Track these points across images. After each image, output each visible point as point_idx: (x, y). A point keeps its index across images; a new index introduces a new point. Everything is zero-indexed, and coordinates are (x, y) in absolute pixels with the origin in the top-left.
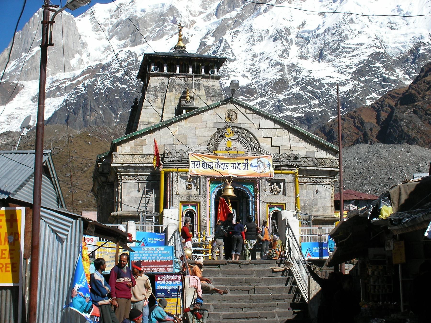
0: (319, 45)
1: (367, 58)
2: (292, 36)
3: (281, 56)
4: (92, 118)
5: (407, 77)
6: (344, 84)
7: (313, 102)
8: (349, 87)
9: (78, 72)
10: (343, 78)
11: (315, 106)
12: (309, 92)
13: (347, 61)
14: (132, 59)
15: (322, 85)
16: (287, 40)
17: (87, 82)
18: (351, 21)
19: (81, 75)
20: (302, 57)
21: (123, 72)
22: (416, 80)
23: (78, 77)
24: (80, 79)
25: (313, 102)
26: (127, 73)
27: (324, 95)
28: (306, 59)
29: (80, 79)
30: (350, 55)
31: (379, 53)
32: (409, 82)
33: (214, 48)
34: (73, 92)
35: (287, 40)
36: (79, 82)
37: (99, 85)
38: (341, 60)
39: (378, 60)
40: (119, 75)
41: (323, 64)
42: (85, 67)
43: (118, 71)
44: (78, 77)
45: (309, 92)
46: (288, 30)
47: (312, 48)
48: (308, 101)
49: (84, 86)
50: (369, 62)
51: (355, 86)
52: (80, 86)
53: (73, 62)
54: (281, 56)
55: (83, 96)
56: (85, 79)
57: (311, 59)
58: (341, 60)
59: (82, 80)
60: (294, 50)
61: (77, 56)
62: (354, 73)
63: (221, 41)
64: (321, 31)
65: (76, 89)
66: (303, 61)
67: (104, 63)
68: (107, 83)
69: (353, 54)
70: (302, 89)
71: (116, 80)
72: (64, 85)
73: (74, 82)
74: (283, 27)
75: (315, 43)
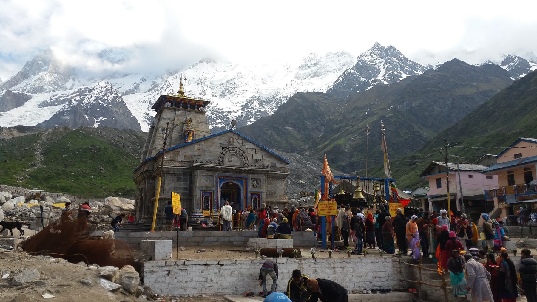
0: (222, 89)
1: (249, 99)
2: (208, 83)
3: (201, 94)
4: (81, 121)
5: (270, 110)
6: (236, 112)
7: (218, 121)
8: (239, 114)
9: (72, 91)
10: (235, 109)
11: (219, 123)
12: (216, 115)
13: (238, 100)
14: (109, 87)
15: (223, 112)
16: (205, 85)
17: (78, 98)
18: (242, 77)
19: (73, 93)
20: (213, 96)
21: (103, 94)
22: (276, 113)
23: (71, 94)
24: (73, 96)
25: (218, 121)
26: (105, 95)
27: (224, 117)
28: (215, 96)
29: (73, 96)
30: (241, 96)
31: (256, 97)
32: (272, 113)
33: (161, 86)
34: (68, 103)
35: (205, 85)
36: (72, 98)
37: (86, 101)
38: (235, 98)
39: (255, 100)
40: (100, 96)
41: (225, 100)
42: (76, 88)
43: (99, 93)
44: (71, 94)
45: (216, 115)
46: (205, 79)
47: (218, 91)
48: (215, 121)
49: (75, 100)
50: (250, 101)
51: (242, 113)
52: (73, 100)
53: (68, 85)
54: (201, 94)
55: (74, 107)
56: (77, 96)
57: (218, 97)
58: (235, 98)
59: (74, 97)
60: (209, 91)
61: (71, 81)
62: (242, 106)
63: (166, 82)
64: (224, 81)
65: (70, 102)
66: (214, 97)
67: (89, 87)
68: (92, 100)
69: (242, 95)
70: (212, 113)
71: (97, 98)
72: (61, 99)
73: (68, 97)
74: (203, 77)
75: (221, 88)
